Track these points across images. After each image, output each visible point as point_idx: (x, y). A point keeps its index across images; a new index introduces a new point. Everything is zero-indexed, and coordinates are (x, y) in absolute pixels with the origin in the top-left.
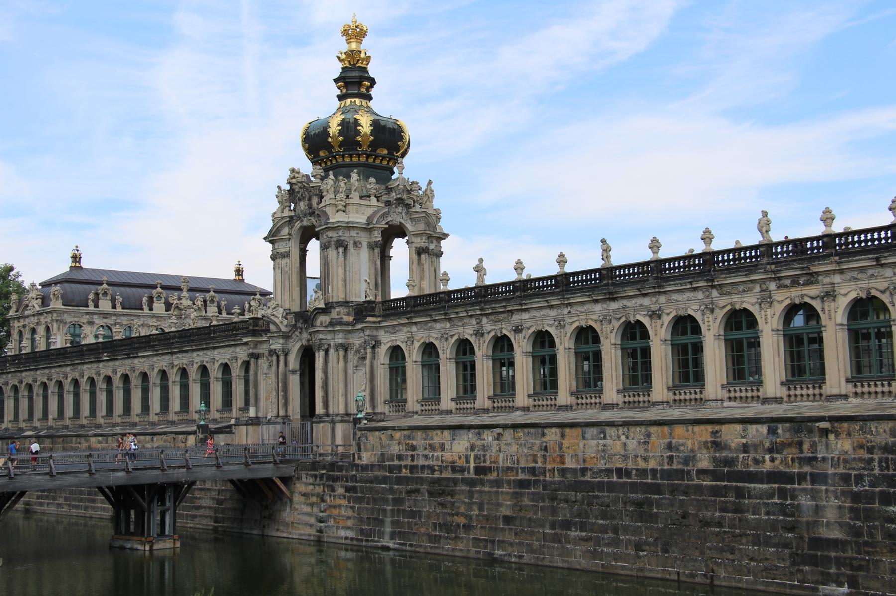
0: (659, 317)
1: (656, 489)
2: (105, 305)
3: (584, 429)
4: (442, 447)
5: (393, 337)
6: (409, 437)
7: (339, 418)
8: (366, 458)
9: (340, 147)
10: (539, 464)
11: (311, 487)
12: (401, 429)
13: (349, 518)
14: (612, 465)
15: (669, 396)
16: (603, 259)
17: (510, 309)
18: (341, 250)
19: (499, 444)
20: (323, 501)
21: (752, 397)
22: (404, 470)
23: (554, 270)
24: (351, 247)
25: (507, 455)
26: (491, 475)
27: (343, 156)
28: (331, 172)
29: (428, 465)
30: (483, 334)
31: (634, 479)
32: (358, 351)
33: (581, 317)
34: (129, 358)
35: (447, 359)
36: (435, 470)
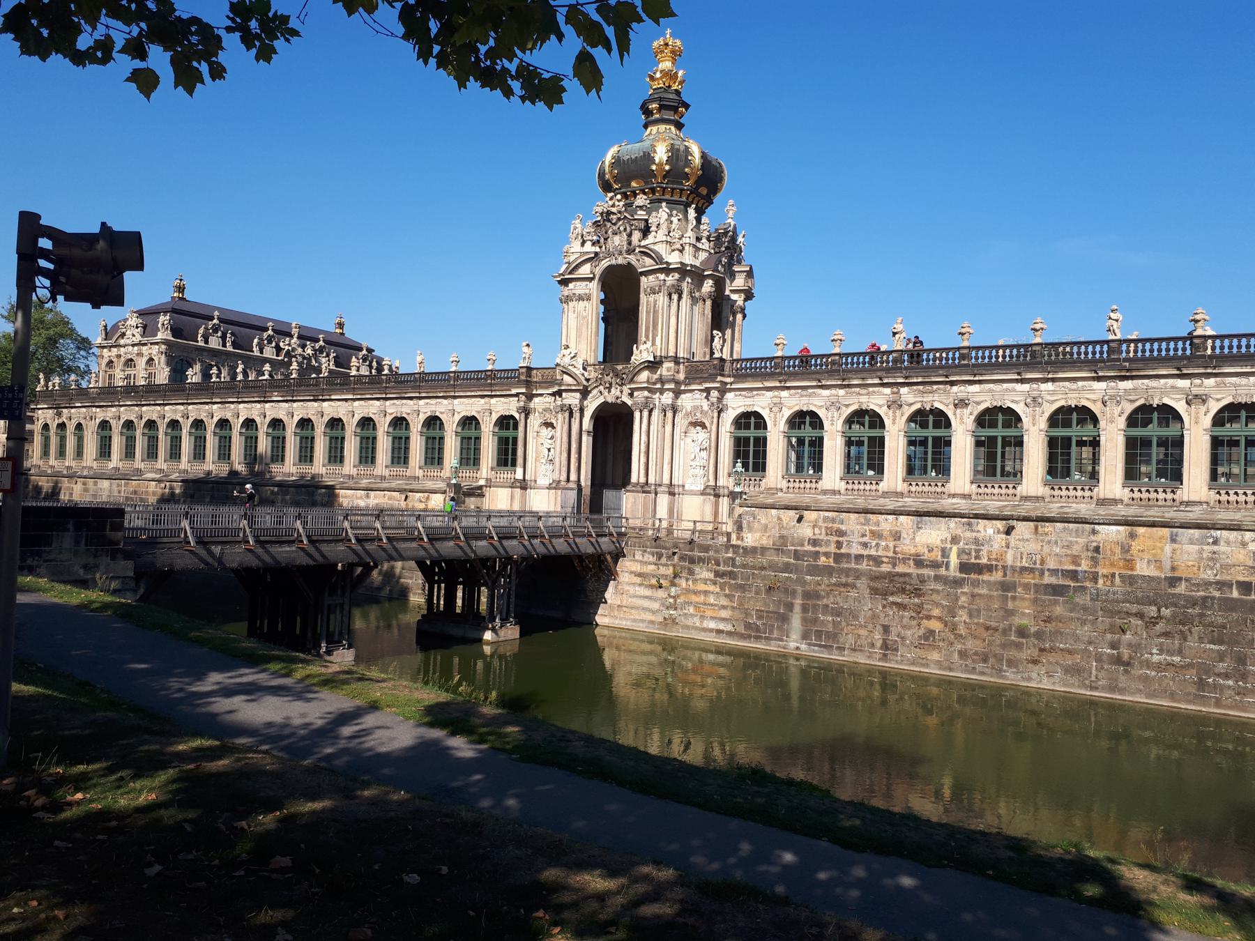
0: (1204, 401)
3: (1175, 530)
4: (897, 536)
5: (749, 401)
8: (750, 539)
9: (664, 177)
10: (1084, 566)
13: (724, 607)
14: (1229, 578)
18: (675, 297)
22: (823, 559)
25: (1022, 553)
34: (315, 400)
36: (883, 562)
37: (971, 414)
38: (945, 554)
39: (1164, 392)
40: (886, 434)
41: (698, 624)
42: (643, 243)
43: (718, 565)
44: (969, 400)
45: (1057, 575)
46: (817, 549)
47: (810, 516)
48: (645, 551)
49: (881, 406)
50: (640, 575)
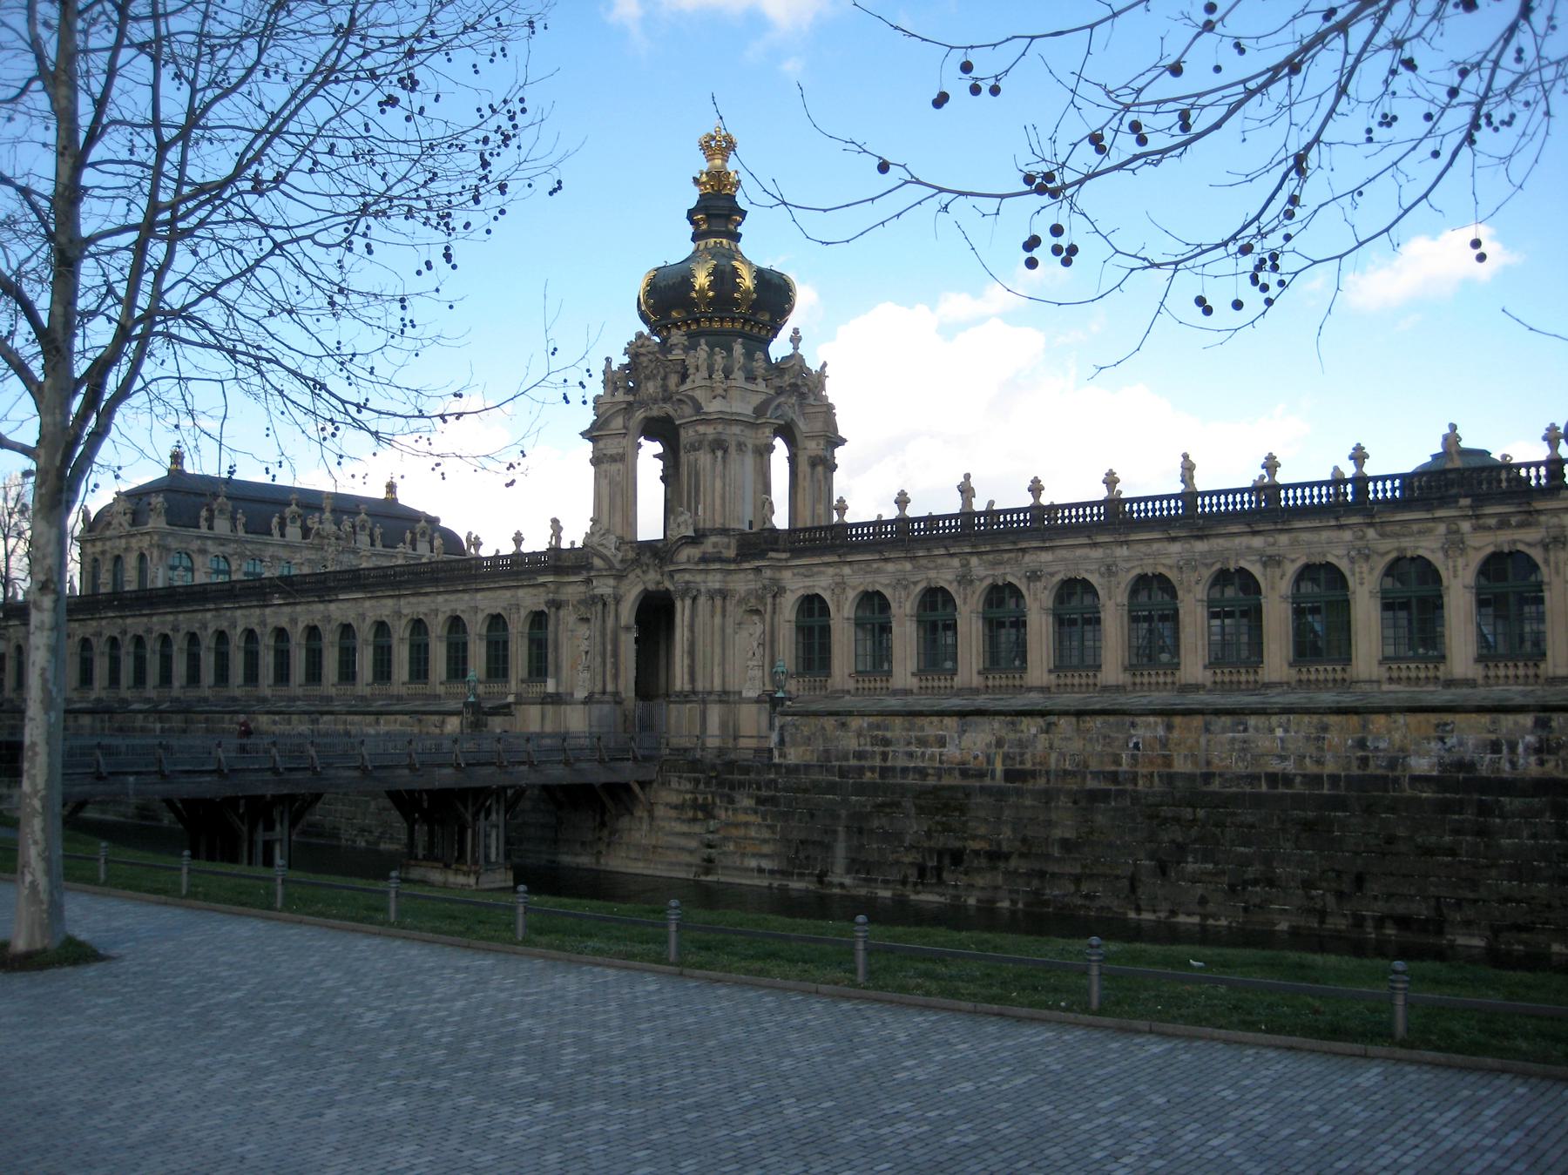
0: (1279, 563)
1: (1338, 803)
2: (222, 526)
3: (1208, 718)
6: (878, 727)
8: (794, 756)
9: (709, 305)
10: (1125, 767)
13: (765, 841)
15: (1291, 674)
18: (719, 454)
21: (1427, 678)
22: (869, 774)
24: (732, 450)
27: (710, 320)
28: (703, 341)
29: (915, 768)
30: (971, 582)
31: (1299, 788)
36: (927, 775)
38: (989, 760)
39: (1240, 554)
40: (957, 616)
41: (738, 864)
42: (683, 388)
43: (759, 788)
46: (863, 763)
47: (855, 723)
48: (680, 777)
49: (950, 583)
50: (676, 807)
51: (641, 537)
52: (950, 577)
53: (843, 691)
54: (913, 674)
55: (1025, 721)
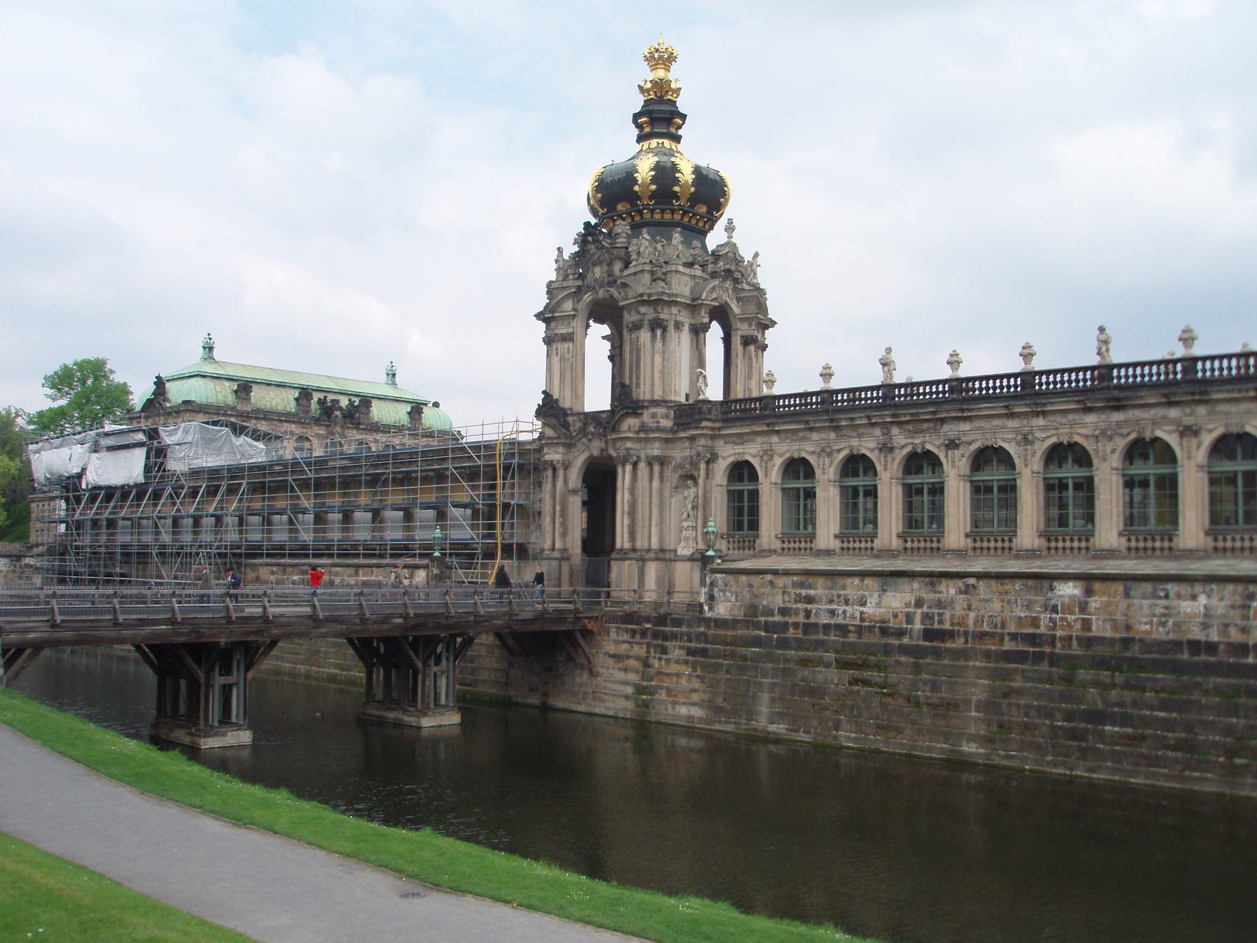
0: (1196, 433)
3: (1129, 583)
5: (739, 449)
7: (652, 555)
8: (722, 610)
9: (651, 198)
10: (1042, 630)
11: (626, 646)
12: (787, 573)
16: (1099, 354)
17: (942, 416)
18: (659, 332)
19: (968, 600)
20: (647, 665)
23: (875, 377)
24: (671, 328)
26: (952, 642)
27: (652, 211)
30: (891, 449)
31: (1223, 656)
32: (680, 466)
33: (1061, 431)
35: (830, 481)
36: (849, 632)
37: (963, 456)
38: (909, 618)
44: (959, 439)
45: (1017, 639)
46: (787, 619)
51: (587, 409)
52: (872, 445)
53: (770, 551)
54: (836, 537)
55: (944, 582)
